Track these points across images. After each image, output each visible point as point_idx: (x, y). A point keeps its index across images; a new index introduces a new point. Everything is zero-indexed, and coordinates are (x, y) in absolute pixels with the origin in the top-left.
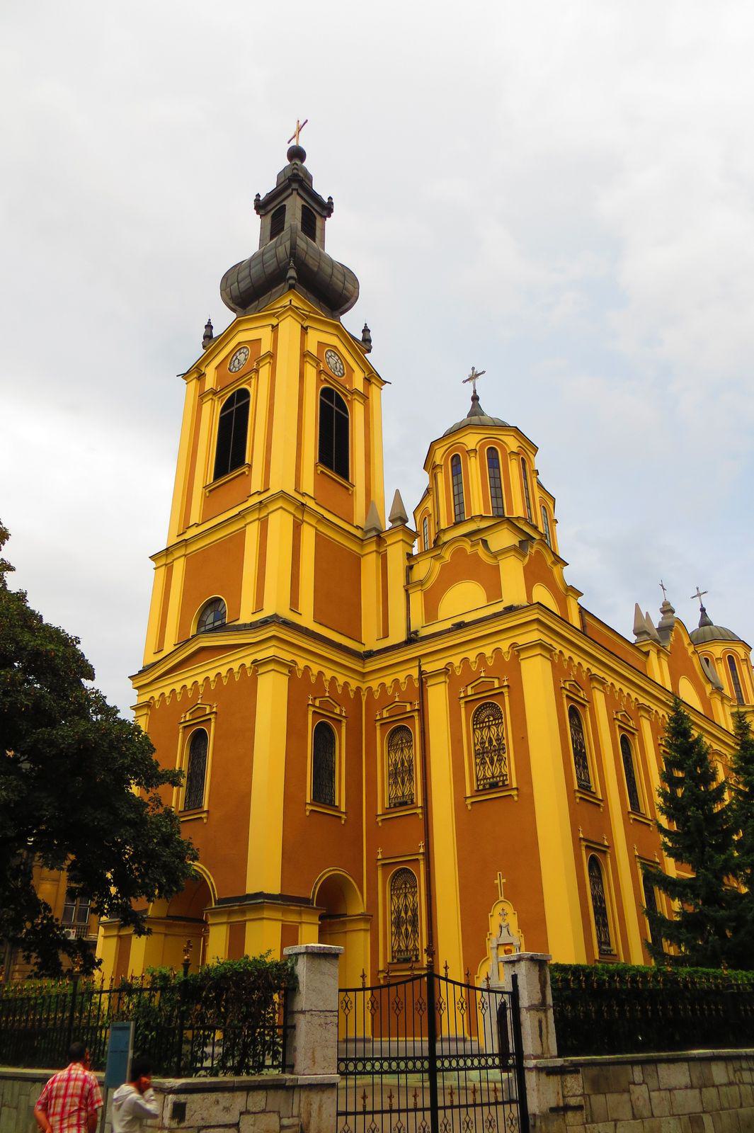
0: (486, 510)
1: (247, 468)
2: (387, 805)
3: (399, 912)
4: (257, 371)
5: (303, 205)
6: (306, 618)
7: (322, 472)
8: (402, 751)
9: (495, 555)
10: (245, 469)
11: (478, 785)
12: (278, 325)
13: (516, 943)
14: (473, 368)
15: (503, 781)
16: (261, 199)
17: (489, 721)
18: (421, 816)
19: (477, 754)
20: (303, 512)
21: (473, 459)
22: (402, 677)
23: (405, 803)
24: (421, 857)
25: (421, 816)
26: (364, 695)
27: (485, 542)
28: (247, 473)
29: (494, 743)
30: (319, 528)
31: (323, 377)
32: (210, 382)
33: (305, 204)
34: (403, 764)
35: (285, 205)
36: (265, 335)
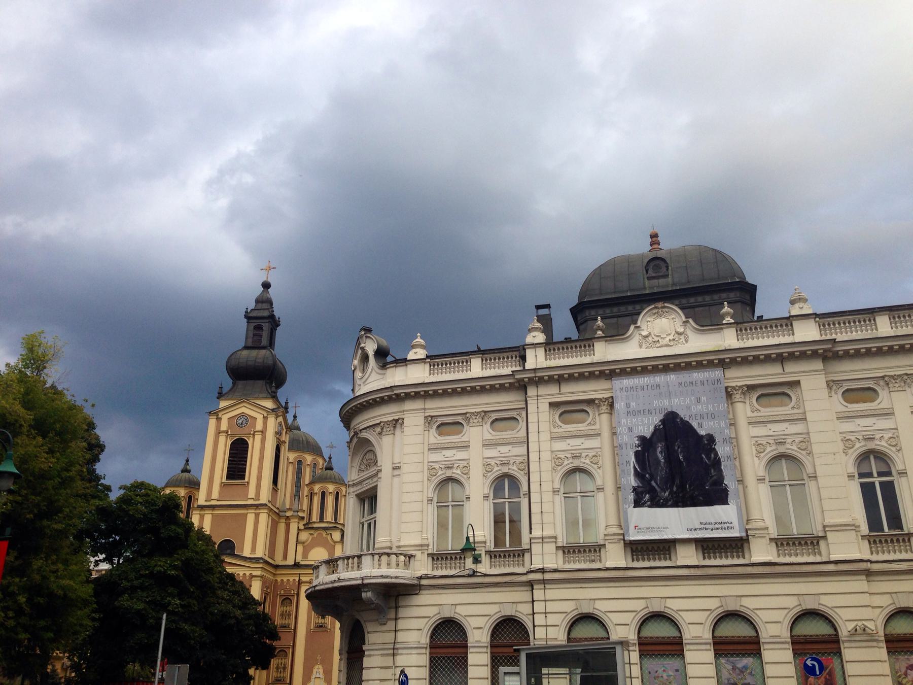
0: (332, 520)
3: (278, 665)
4: (254, 435)
6: (267, 558)
8: (286, 607)
9: (335, 542)
12: (267, 417)
13: (321, 677)
14: (332, 443)
22: (291, 579)
23: (285, 627)
27: (331, 534)
32: (224, 427)
34: (286, 612)
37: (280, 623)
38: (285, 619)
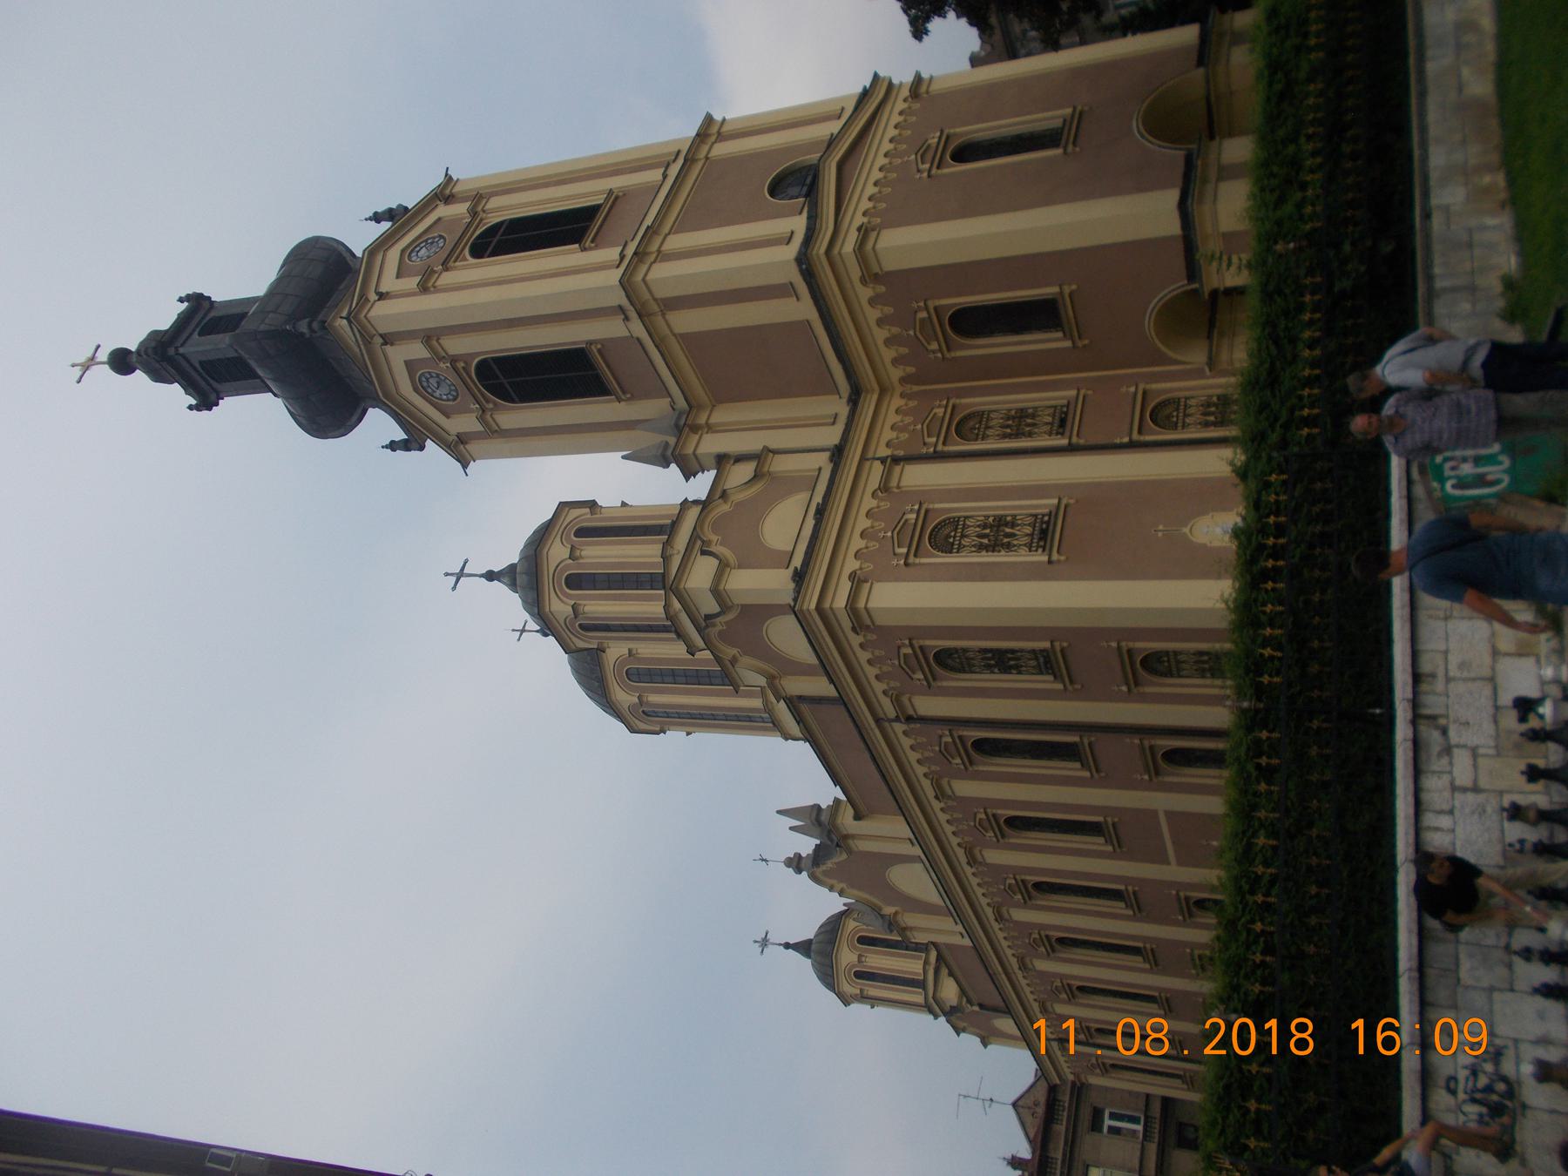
1: (593, 347)
5: (199, 335)
16: (194, 402)
28: (599, 346)
33: (196, 333)
35: (201, 363)
36: (398, 356)
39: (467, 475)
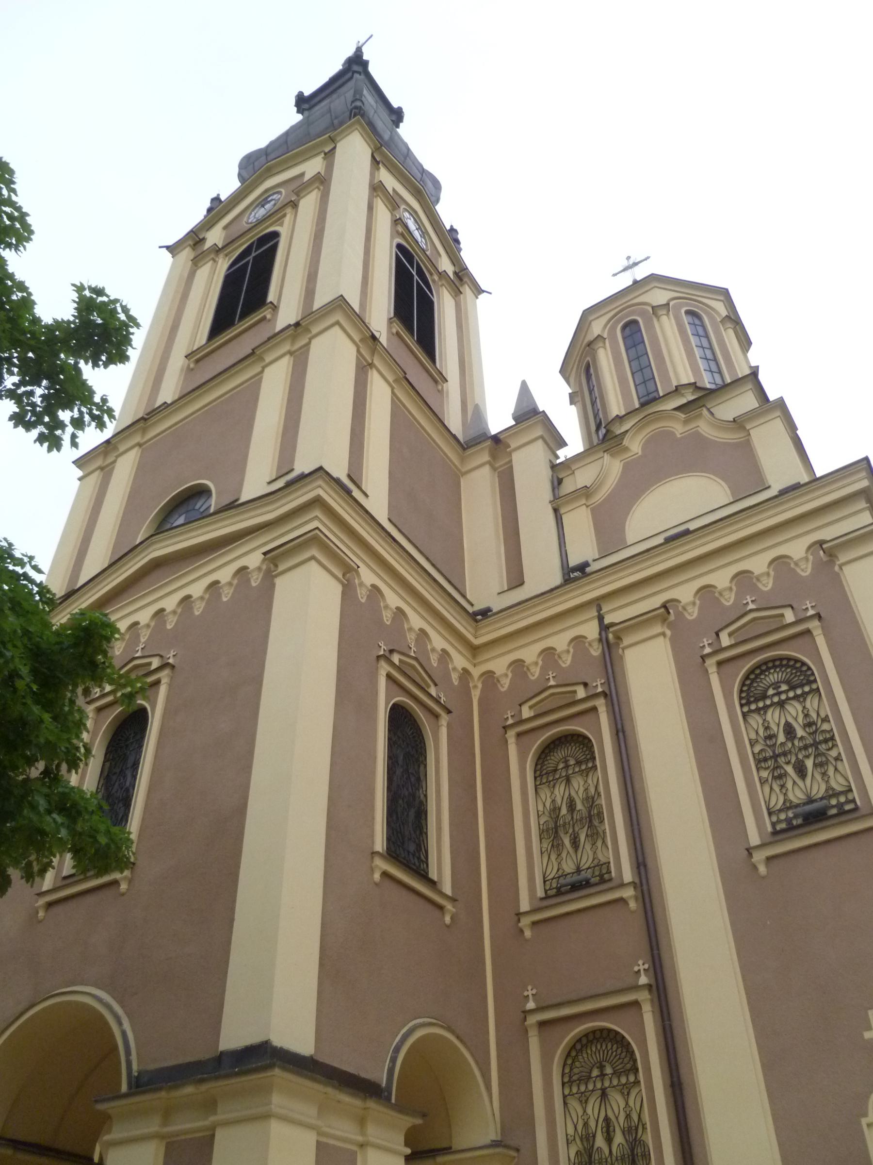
2: (540, 893)
3: (588, 1138)
4: (294, 205)
7: (398, 333)
8: (568, 780)
10: (267, 313)
11: (773, 825)
15: (840, 806)
17: (779, 694)
18: (633, 905)
19: (760, 761)
20: (373, 352)
21: (664, 319)
23: (586, 884)
24: (643, 997)
25: (633, 905)
26: (475, 687)
29: (800, 732)
30: (396, 391)
31: (400, 229)
37: (552, 873)
38: (575, 843)
39: (160, 247)
